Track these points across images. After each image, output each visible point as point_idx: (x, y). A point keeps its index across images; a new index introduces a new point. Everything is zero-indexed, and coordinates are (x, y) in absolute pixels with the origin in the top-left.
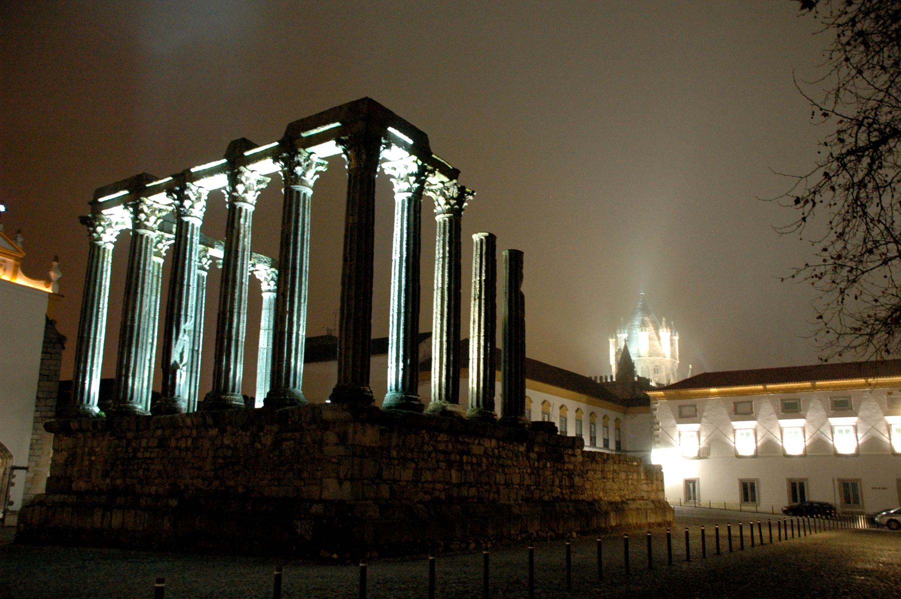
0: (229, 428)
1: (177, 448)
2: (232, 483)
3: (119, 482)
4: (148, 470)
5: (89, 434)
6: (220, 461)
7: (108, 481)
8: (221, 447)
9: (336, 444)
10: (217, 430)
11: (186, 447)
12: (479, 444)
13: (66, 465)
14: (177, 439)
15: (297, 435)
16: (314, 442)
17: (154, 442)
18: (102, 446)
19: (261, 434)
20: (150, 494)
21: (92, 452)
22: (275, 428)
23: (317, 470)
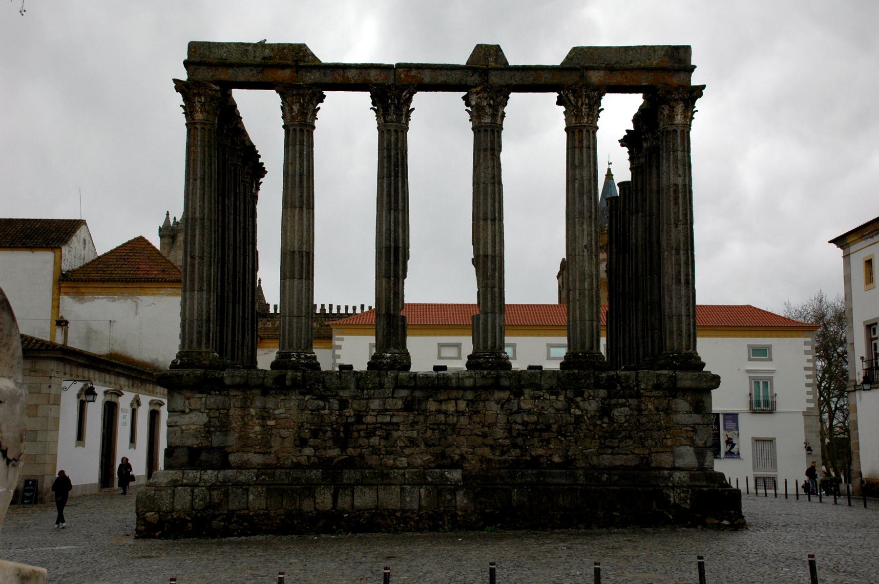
0: (527, 391)
1: (439, 412)
2: (541, 451)
3: (334, 452)
6: (518, 427)
7: (308, 451)
8: (516, 412)
9: (690, 412)
10: (508, 393)
11: (457, 411)
13: (209, 432)
14: (441, 402)
15: (633, 402)
16: (657, 409)
17: (400, 404)
19: (579, 399)
20: (404, 468)
22: (602, 393)
23: (665, 438)
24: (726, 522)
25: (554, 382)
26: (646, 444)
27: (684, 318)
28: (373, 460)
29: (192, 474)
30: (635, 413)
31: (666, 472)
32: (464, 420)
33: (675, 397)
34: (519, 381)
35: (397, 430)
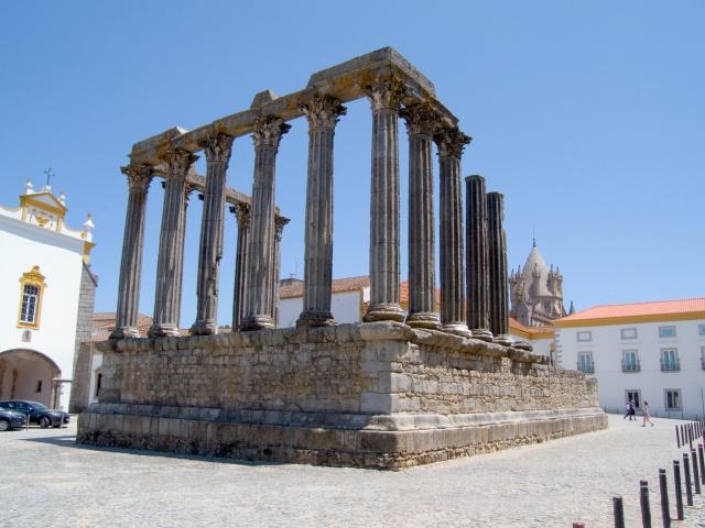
0: (264, 348)
1: (214, 365)
2: (269, 396)
3: (163, 394)
4: (188, 384)
5: (135, 353)
6: (257, 376)
7: (152, 393)
12: (481, 361)
15: (334, 352)
17: (194, 360)
18: (148, 361)
21: (138, 368)
22: (311, 346)
24: (381, 464)
25: (282, 340)
26: (341, 390)
27: (377, 274)
28: (180, 401)
29: (104, 405)
30: (334, 363)
31: (348, 416)
32: (227, 370)
33: (363, 347)
34: (259, 339)
35: (192, 378)
